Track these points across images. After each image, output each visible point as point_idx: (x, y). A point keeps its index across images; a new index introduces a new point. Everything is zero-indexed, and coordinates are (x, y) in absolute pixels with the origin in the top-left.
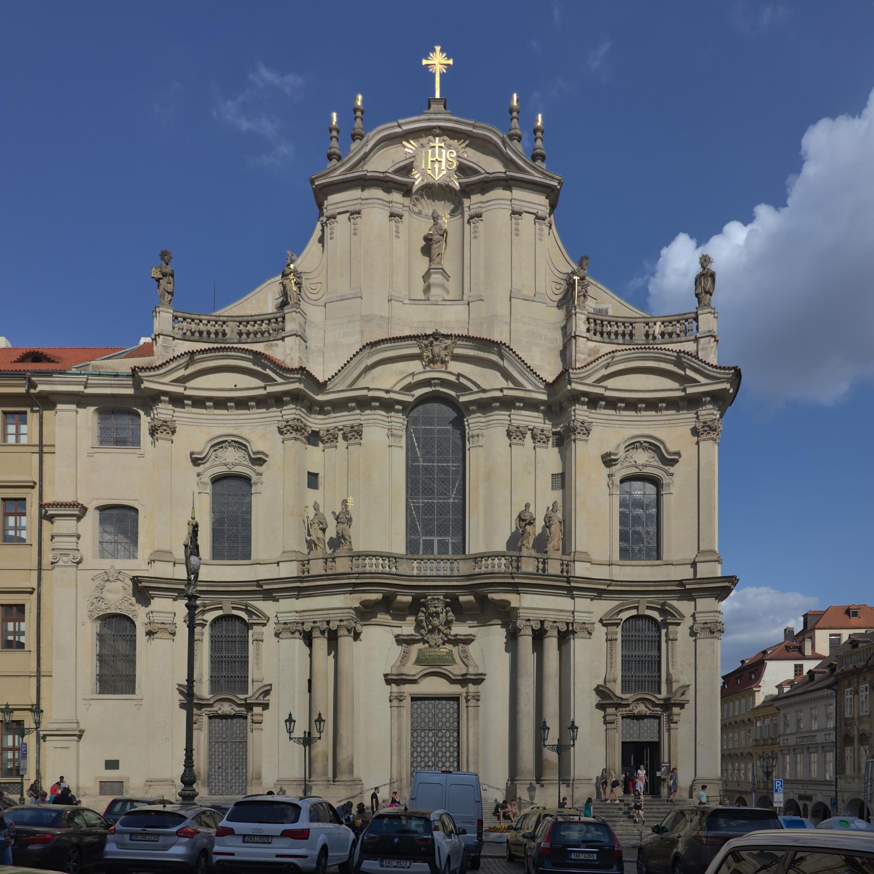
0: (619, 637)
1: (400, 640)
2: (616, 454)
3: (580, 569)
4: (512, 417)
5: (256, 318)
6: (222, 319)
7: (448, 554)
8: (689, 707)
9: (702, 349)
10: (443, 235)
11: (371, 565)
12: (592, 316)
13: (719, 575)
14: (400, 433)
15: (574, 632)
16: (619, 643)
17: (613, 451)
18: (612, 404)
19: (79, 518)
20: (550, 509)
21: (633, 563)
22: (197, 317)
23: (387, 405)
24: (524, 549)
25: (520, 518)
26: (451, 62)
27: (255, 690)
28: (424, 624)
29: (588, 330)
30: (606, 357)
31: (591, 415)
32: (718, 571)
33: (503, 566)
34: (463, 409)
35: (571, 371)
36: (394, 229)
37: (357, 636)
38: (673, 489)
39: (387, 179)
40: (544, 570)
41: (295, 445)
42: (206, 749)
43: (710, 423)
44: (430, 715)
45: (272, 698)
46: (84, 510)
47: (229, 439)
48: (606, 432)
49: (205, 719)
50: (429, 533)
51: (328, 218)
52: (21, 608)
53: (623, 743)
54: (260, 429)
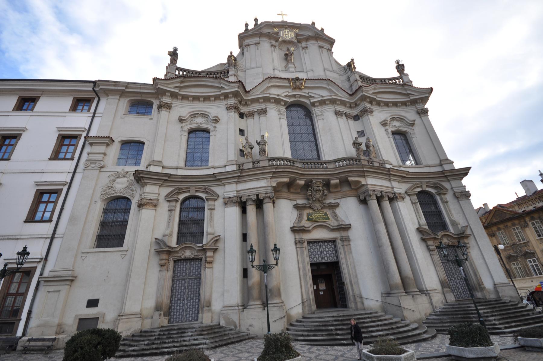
18: (379, 103)
19: (108, 145)
23: (278, 101)
27: (209, 240)
41: (234, 115)
44: (319, 253)
45: (220, 245)
47: (200, 113)
54: (217, 109)
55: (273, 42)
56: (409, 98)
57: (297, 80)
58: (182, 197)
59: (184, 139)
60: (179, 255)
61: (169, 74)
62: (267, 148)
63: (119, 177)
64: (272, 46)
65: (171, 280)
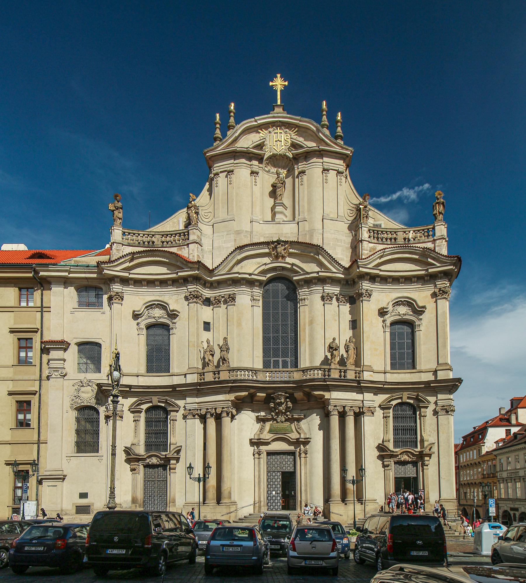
0: (391, 415)
1: (259, 420)
3: (367, 376)
4: (325, 288)
5: (172, 233)
6: (151, 233)
7: (288, 368)
8: (434, 457)
9: (438, 246)
10: (283, 184)
11: (241, 375)
12: (371, 228)
13: (451, 378)
14: (258, 298)
15: (363, 413)
17: (385, 306)
19: (65, 350)
20: (348, 341)
21: (399, 371)
22: (137, 232)
24: (332, 365)
25: (330, 347)
26: (286, 83)
29: (370, 237)
30: (380, 252)
31: (372, 286)
32: (451, 375)
33: (320, 375)
34: (296, 284)
35: (358, 260)
36: (254, 180)
37: (233, 417)
38: (422, 328)
39: (249, 152)
40: (345, 376)
42: (142, 485)
43: (443, 289)
46: (69, 344)
48: (380, 296)
49: (142, 467)
50: (276, 355)
51: (215, 175)
52: (29, 403)
53: (395, 478)
55: (255, 163)
58: (145, 407)
59: (143, 339)
60: (147, 461)
62: (230, 356)
63: (83, 386)
64: (252, 173)
65: (142, 482)
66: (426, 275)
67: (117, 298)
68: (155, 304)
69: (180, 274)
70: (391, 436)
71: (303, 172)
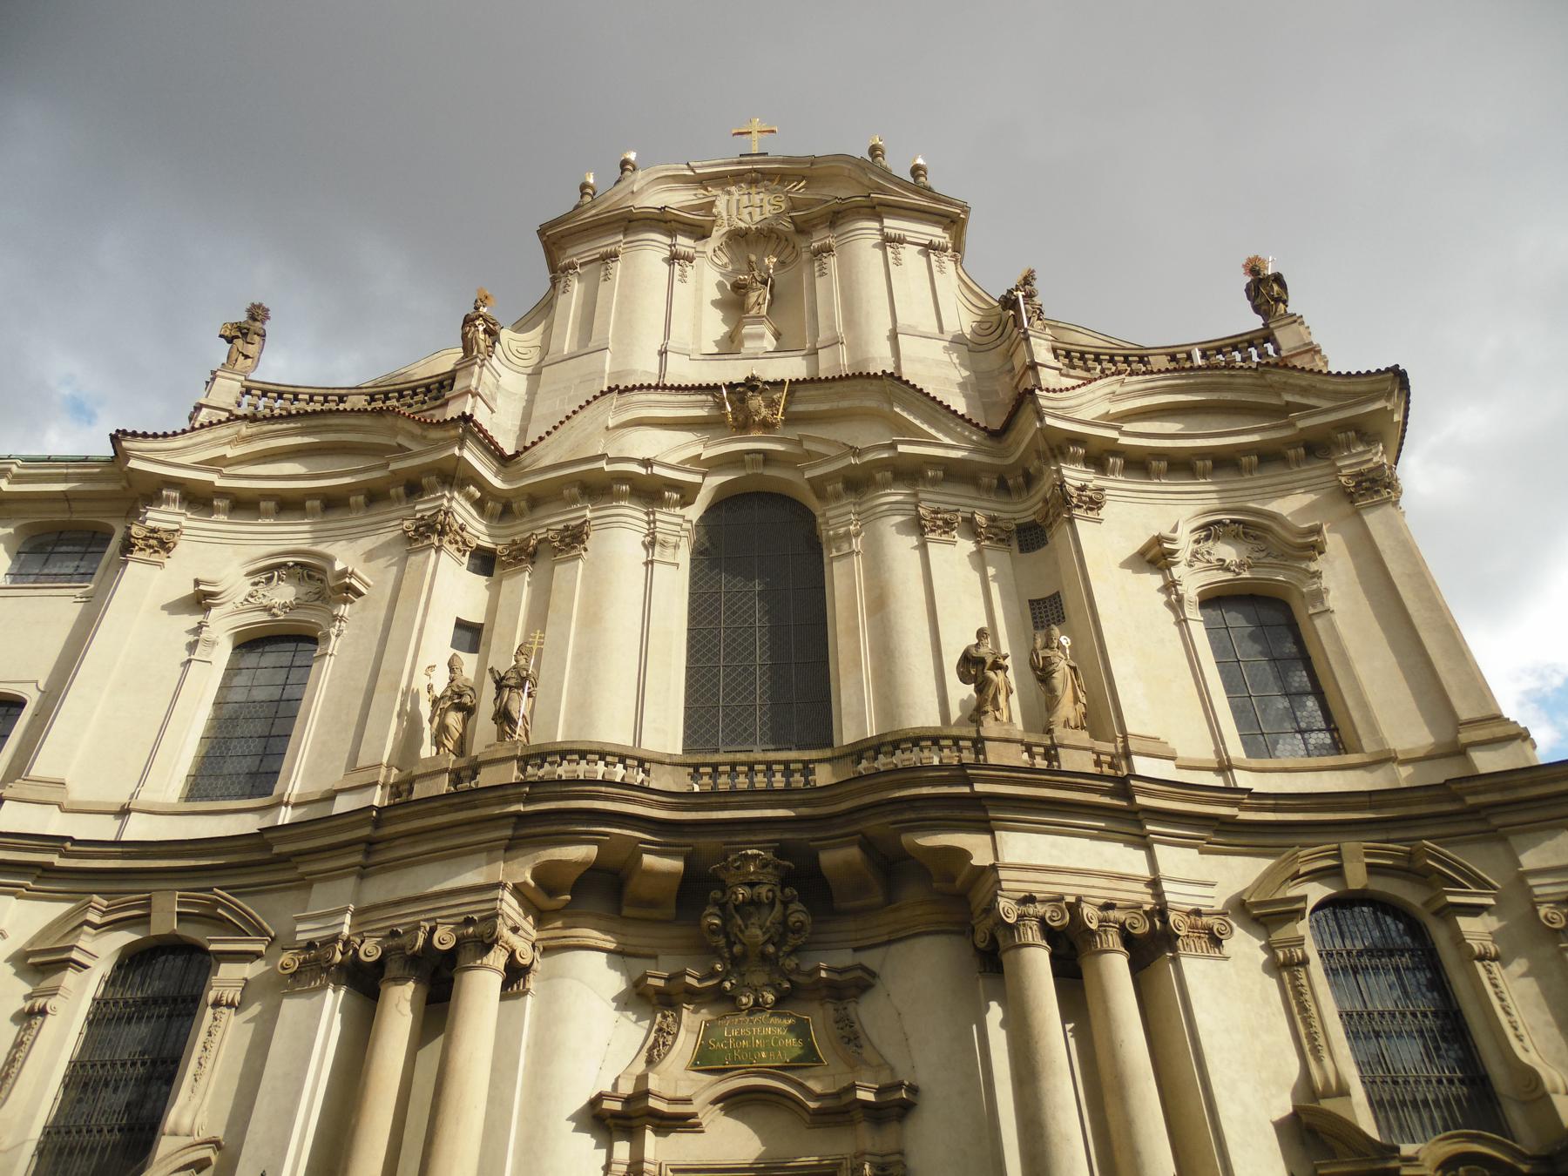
0: (1311, 950)
2: (1173, 541)
16: (1316, 967)
17: (1166, 532)
23: (650, 491)
28: (722, 942)
47: (290, 560)
55: (684, 243)
56: (1292, 425)
57: (754, 388)
61: (205, 410)
66: (1290, 443)
67: (151, 547)
68: (284, 565)
69: (393, 466)
70: (1344, 1061)
71: (828, 250)
